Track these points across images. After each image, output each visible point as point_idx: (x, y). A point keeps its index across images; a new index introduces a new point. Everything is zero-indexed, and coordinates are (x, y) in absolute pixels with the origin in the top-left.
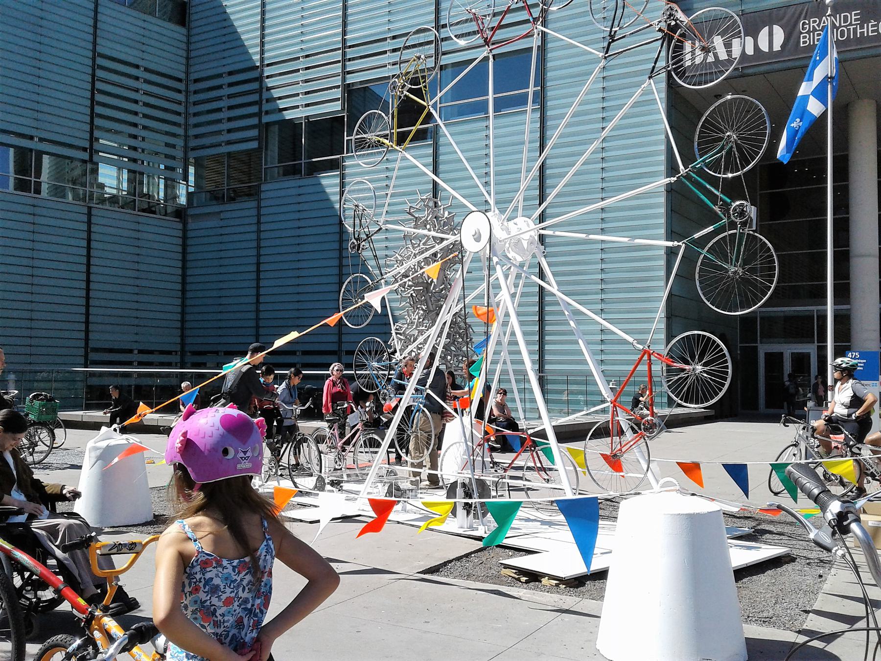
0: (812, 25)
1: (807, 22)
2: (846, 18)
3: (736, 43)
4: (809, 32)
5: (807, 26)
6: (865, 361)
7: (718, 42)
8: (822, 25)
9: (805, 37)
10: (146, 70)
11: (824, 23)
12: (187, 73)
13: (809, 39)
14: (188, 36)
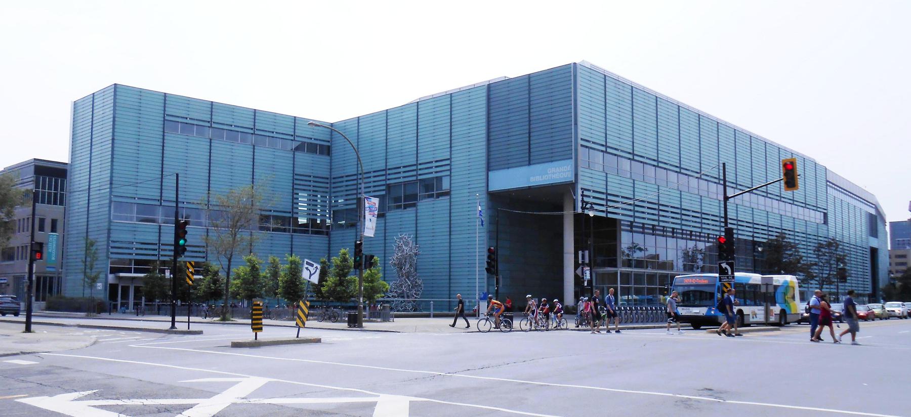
10: (314, 177)
12: (331, 175)
14: (331, 160)
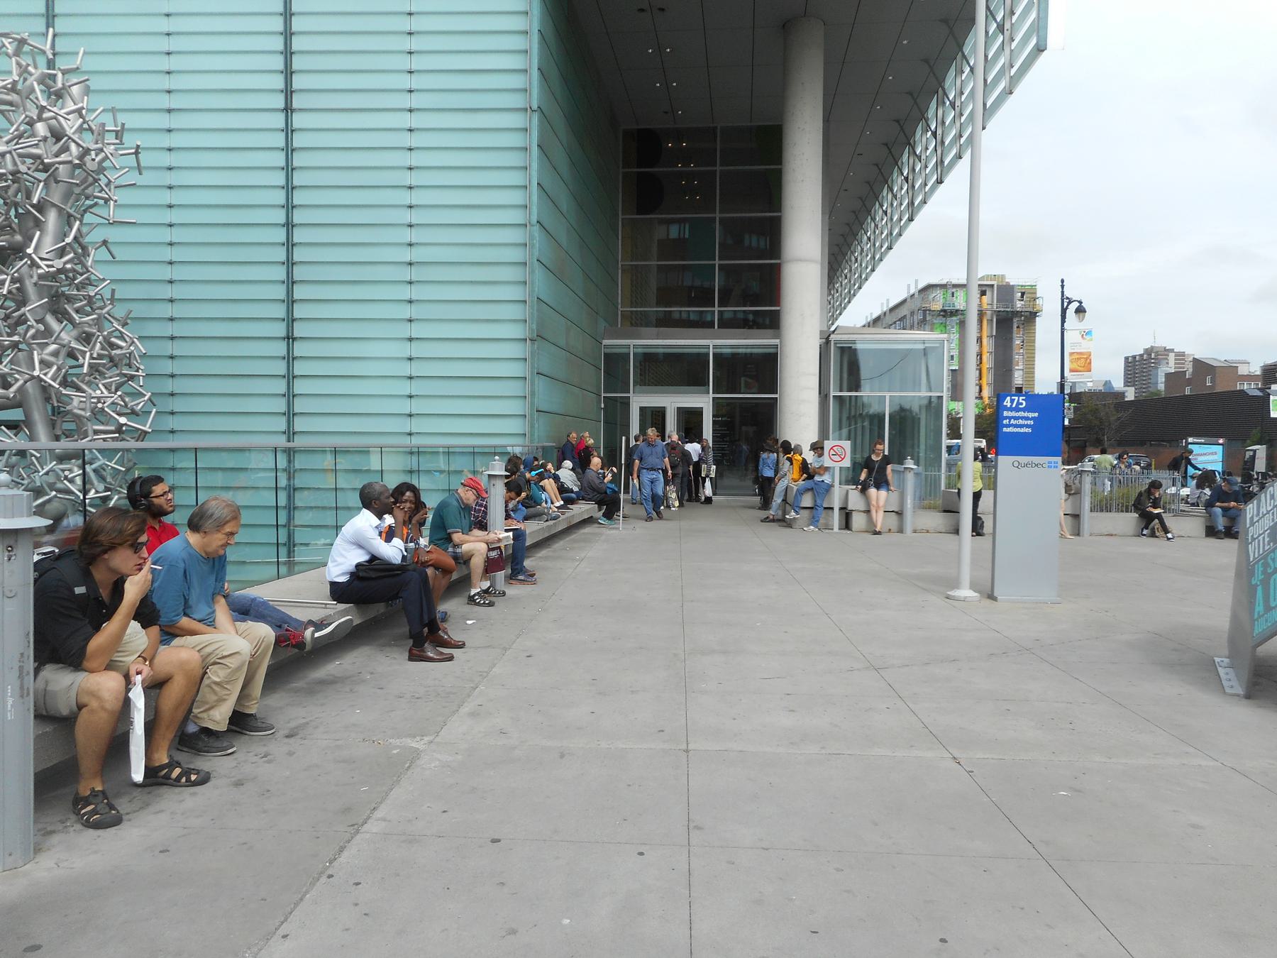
6: (1036, 415)
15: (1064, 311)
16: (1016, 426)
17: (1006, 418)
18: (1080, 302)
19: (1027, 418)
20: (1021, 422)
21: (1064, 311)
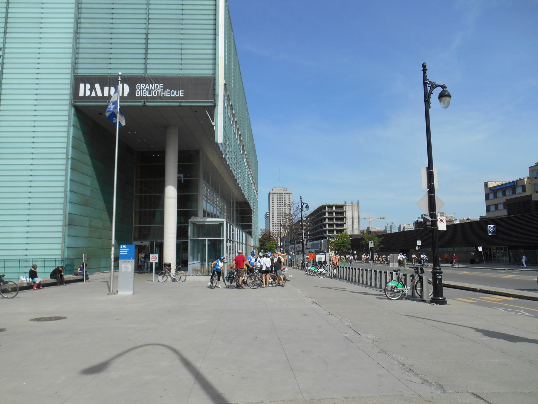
0: (142, 87)
1: (140, 85)
2: (157, 86)
3: (106, 89)
4: (140, 90)
5: (140, 87)
6: (128, 250)
7: (97, 86)
8: (146, 87)
9: (138, 92)
11: (147, 87)
13: (140, 93)
15: (302, 207)
16: (123, 252)
17: (121, 251)
18: (307, 204)
19: (126, 251)
20: (124, 251)
21: (302, 207)
